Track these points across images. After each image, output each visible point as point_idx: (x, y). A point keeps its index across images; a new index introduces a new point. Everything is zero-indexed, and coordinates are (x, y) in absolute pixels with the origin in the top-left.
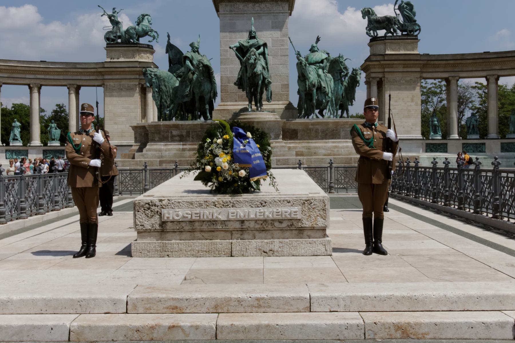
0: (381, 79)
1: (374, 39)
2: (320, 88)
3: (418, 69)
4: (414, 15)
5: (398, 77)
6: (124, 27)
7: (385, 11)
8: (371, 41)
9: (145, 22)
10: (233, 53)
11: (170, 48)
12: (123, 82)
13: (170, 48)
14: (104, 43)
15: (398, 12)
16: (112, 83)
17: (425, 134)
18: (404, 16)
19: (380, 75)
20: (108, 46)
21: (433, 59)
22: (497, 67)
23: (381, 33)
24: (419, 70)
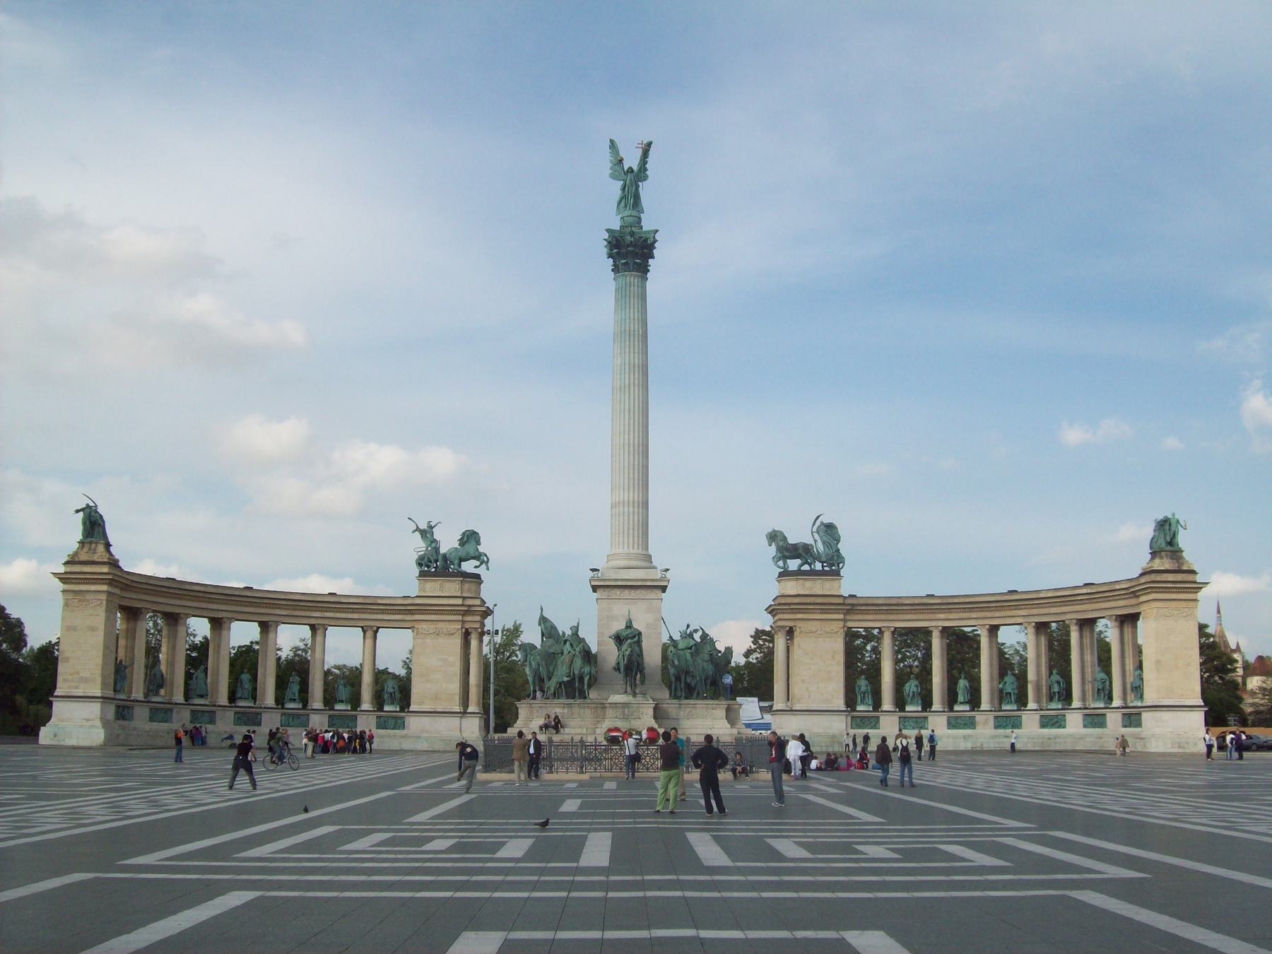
0: (791, 628)
1: (785, 574)
2: (687, 673)
3: (841, 616)
4: (838, 541)
5: (813, 626)
6: (443, 550)
7: (799, 534)
8: (781, 575)
9: (473, 543)
10: (612, 642)
11: (543, 620)
12: (441, 625)
13: (543, 620)
14: (417, 571)
15: (816, 536)
16: (424, 626)
17: (851, 702)
18: (824, 543)
19: (790, 624)
20: (423, 574)
21: (862, 602)
22: (942, 616)
23: (793, 564)
24: (841, 616)
